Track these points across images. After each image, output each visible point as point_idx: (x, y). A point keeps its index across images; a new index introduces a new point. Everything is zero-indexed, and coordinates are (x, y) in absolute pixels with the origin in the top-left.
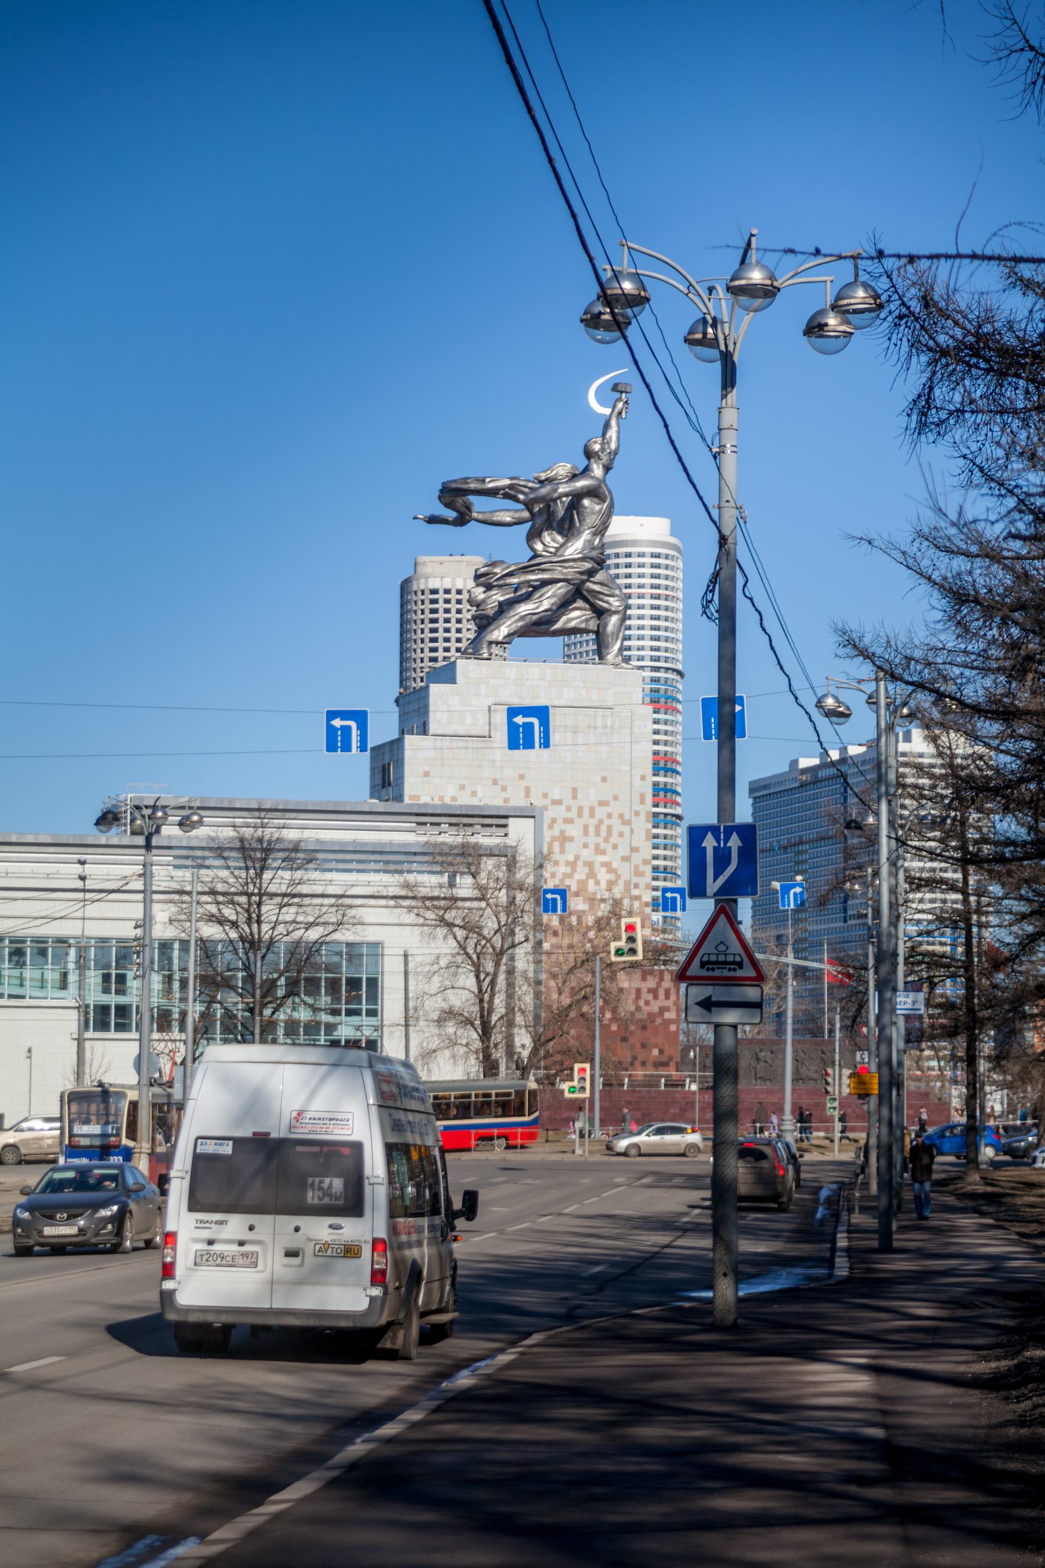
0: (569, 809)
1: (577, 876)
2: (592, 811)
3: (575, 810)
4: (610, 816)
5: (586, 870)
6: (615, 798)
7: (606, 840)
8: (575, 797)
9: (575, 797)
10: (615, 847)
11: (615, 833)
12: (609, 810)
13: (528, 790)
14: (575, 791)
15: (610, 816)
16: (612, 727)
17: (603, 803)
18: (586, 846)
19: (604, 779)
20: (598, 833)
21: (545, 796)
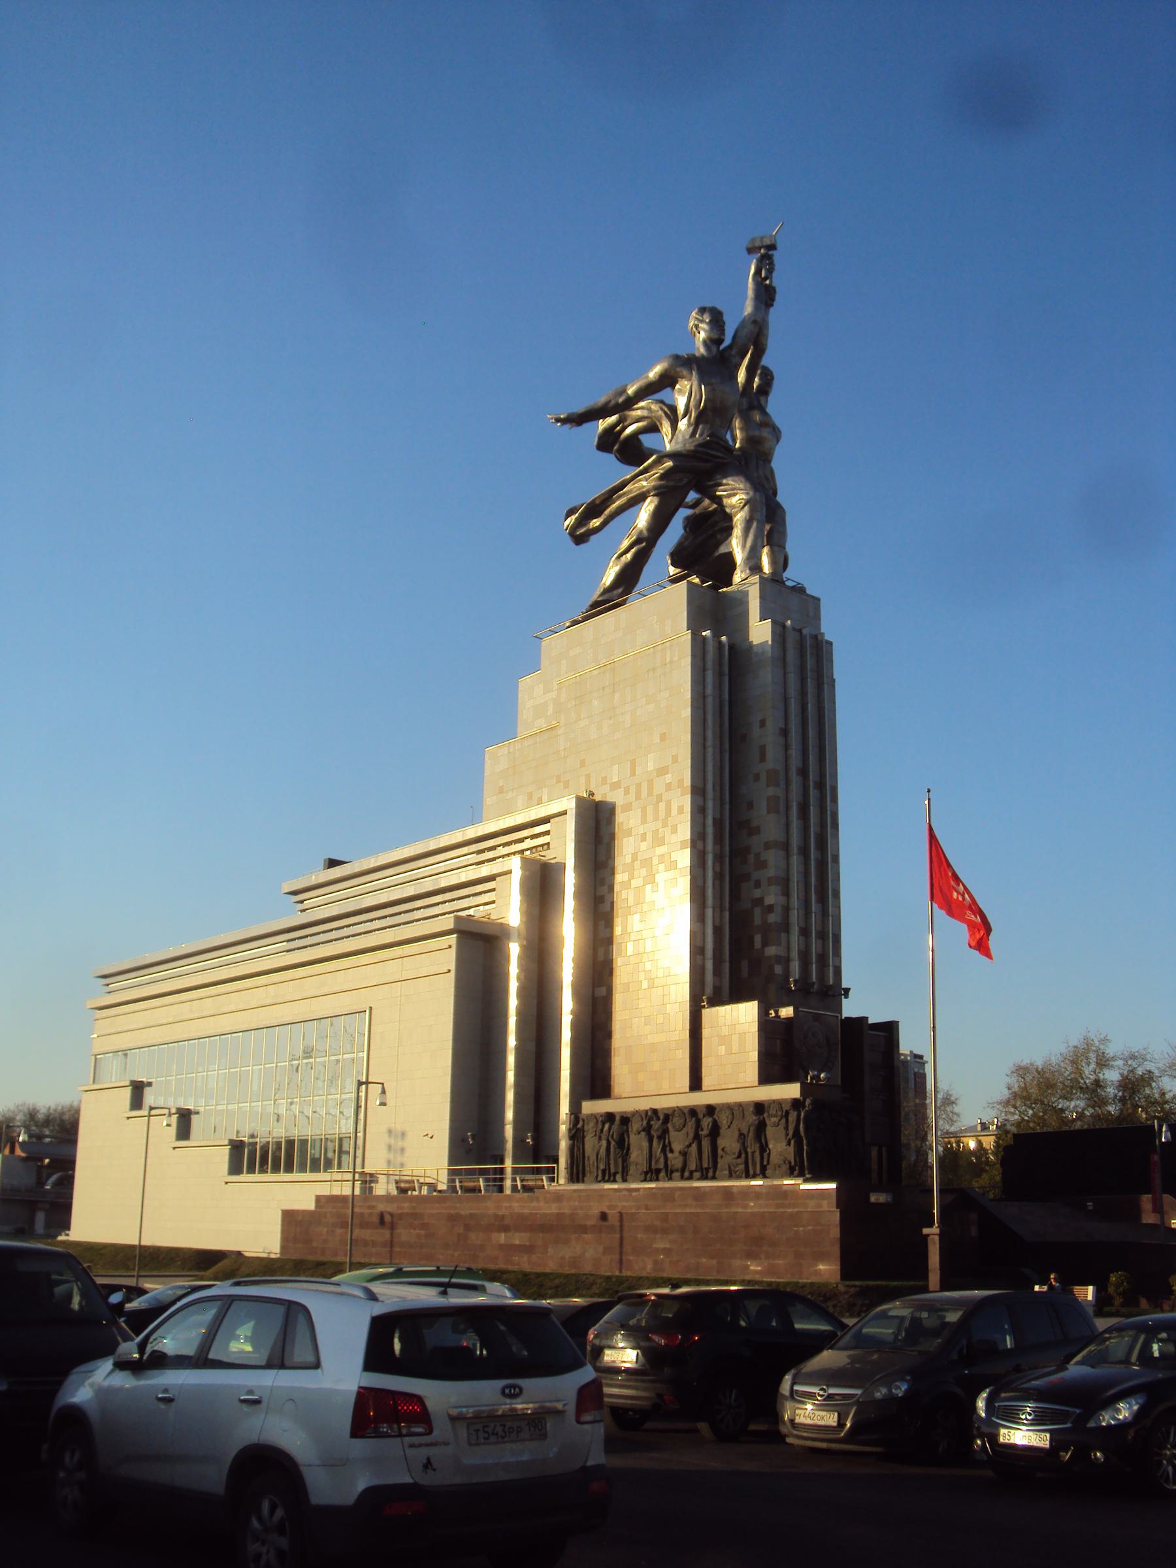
0: (627, 792)
1: (634, 884)
2: (650, 783)
3: (633, 790)
4: (669, 787)
5: (644, 872)
6: (675, 759)
7: (665, 825)
8: (633, 773)
9: (633, 773)
10: (674, 830)
11: (674, 811)
12: (668, 778)
13: (588, 776)
14: (633, 764)
15: (669, 787)
16: (671, 662)
17: (662, 771)
18: (644, 838)
19: (663, 737)
20: (656, 818)
21: (604, 779)
